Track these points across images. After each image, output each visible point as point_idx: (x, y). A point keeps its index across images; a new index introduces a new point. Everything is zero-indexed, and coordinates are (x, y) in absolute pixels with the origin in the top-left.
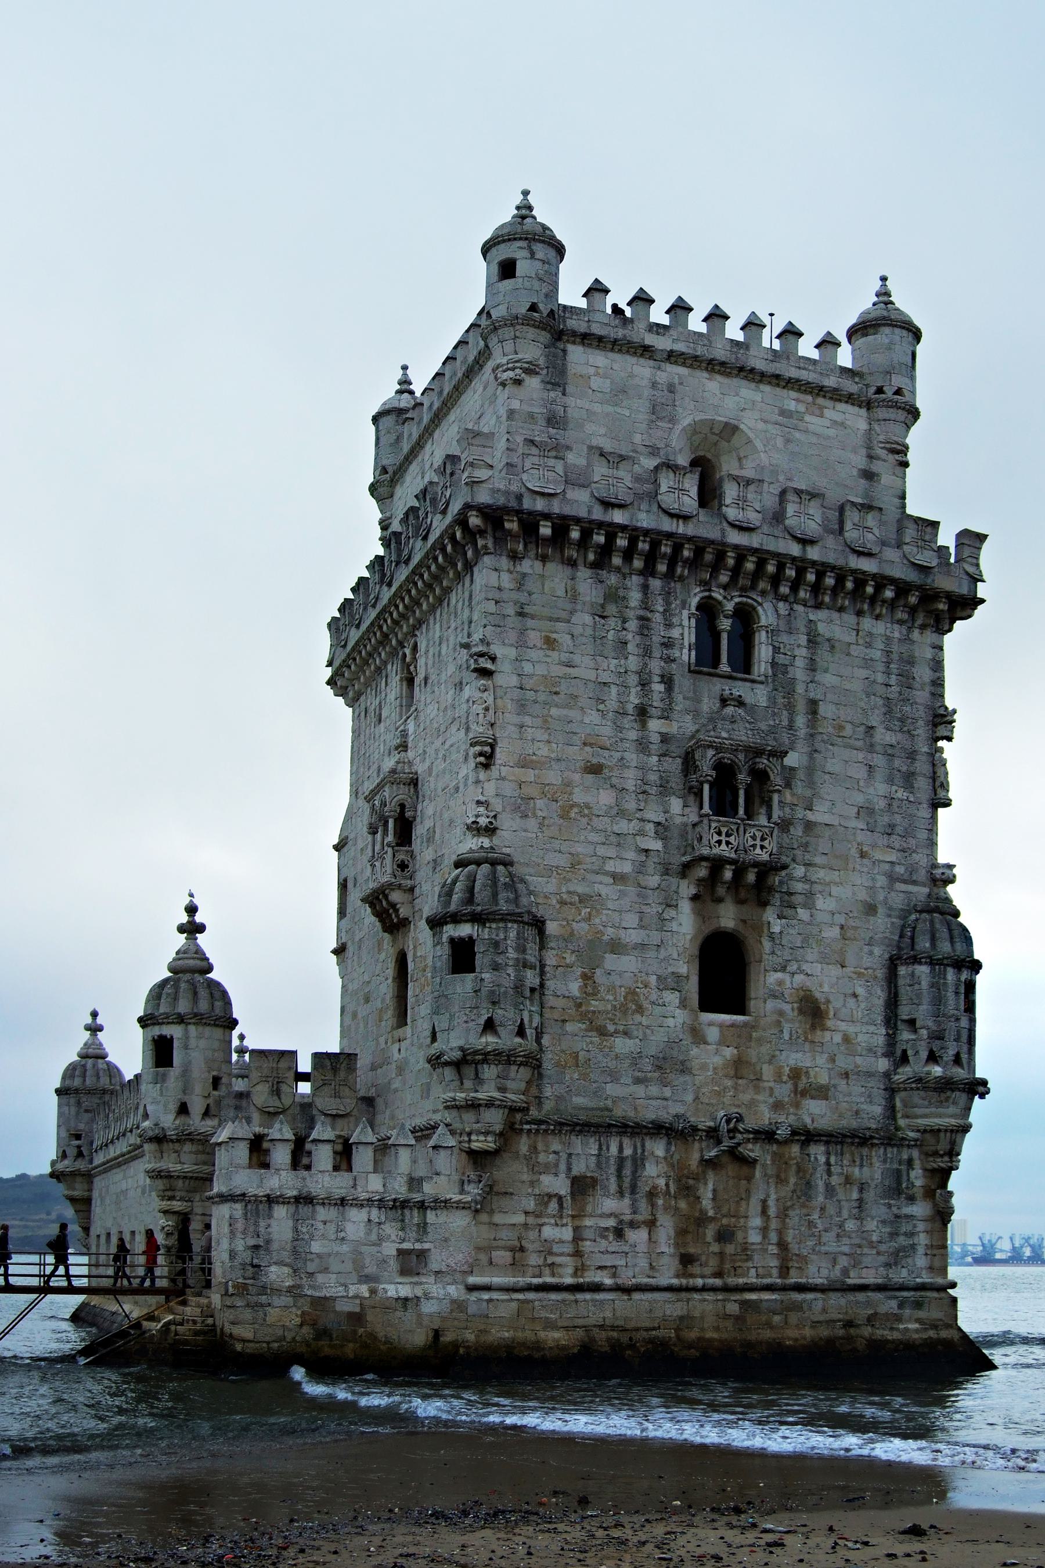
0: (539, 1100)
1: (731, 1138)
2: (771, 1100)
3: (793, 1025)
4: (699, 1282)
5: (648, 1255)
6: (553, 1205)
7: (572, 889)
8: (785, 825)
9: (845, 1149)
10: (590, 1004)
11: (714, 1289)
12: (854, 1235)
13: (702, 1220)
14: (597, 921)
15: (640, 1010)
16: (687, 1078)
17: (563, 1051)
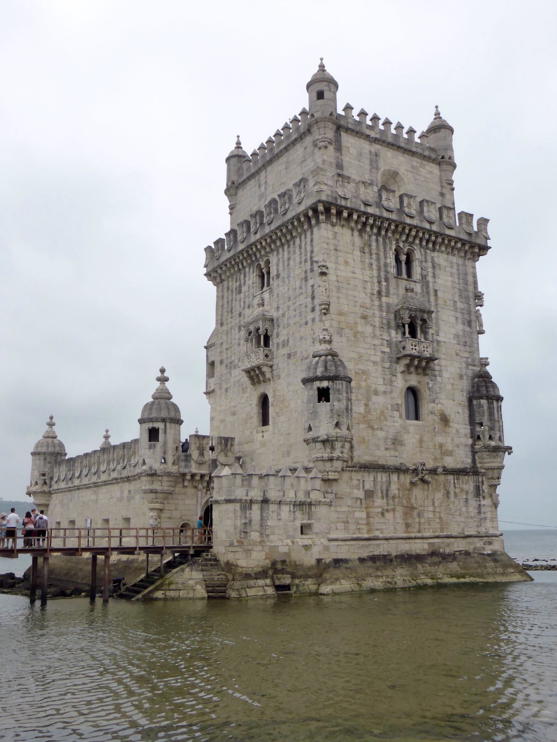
0: (352, 458)
2: (433, 457)
3: (438, 426)
4: (413, 535)
11: (418, 538)
13: (413, 508)
14: (368, 381)
15: (386, 419)
16: (403, 448)
17: (359, 436)
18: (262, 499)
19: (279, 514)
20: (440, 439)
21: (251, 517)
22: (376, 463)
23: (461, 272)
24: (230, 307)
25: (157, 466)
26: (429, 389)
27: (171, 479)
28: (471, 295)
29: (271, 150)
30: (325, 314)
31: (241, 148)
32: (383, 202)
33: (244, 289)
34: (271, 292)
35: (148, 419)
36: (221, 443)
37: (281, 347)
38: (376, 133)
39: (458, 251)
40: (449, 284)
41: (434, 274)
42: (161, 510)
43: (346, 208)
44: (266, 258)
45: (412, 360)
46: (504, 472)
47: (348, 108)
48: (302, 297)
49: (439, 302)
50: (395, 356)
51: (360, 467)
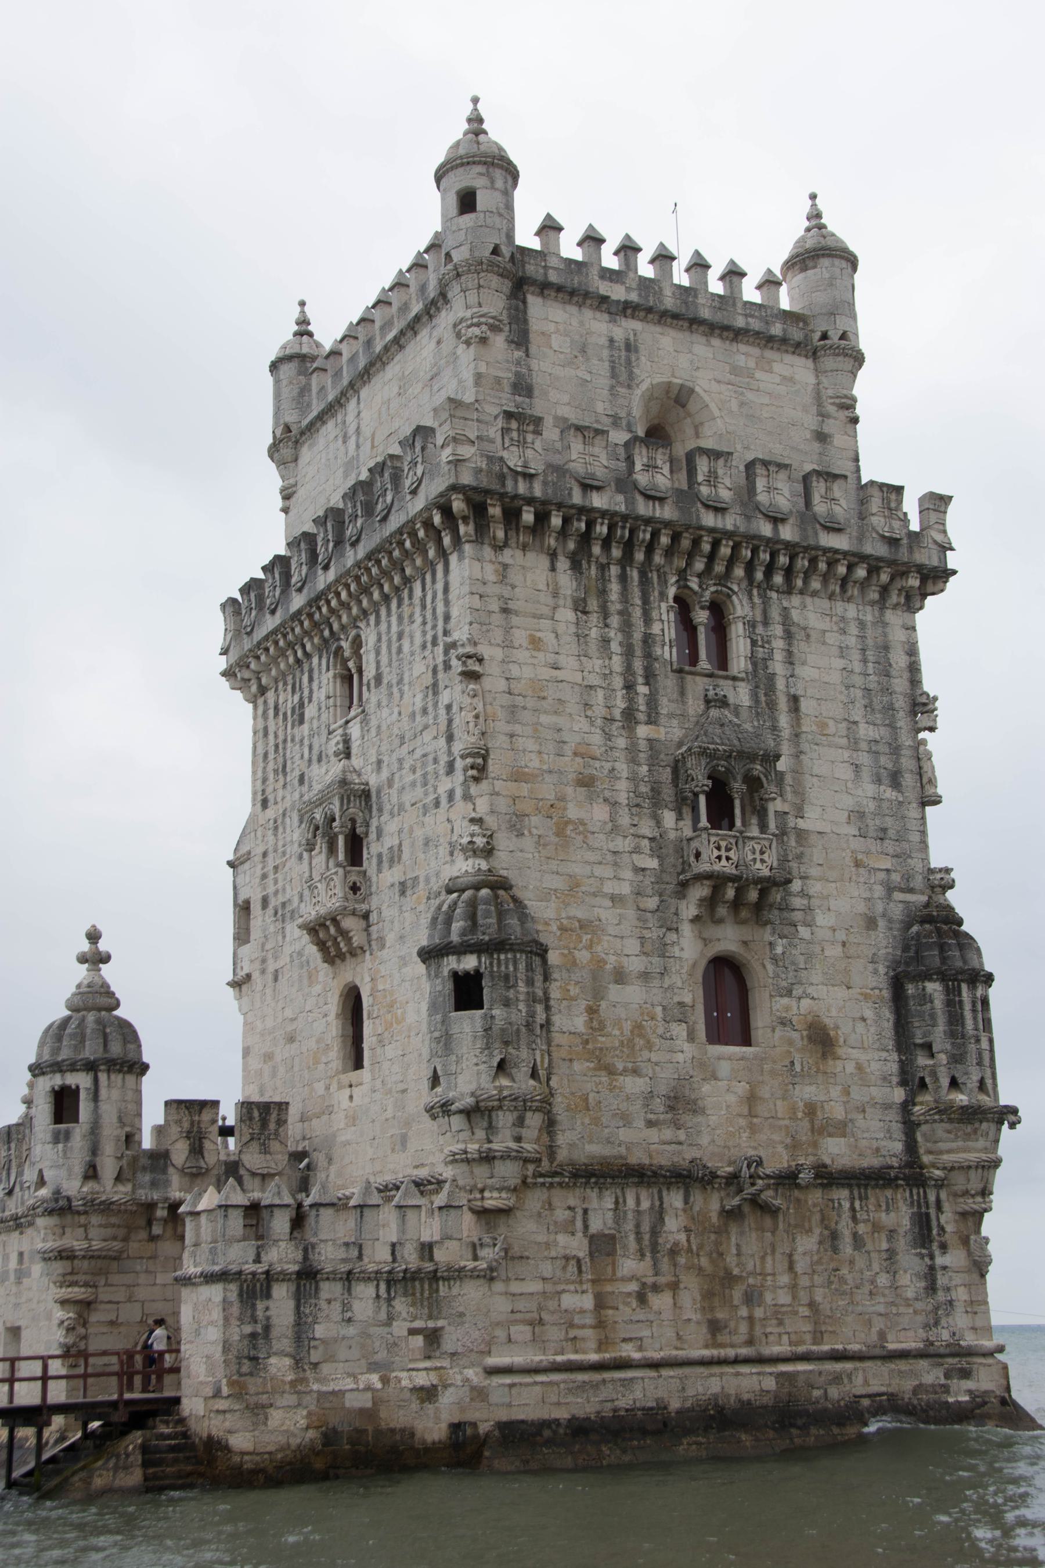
0: (552, 1151)
1: (753, 1184)
4: (731, 1353)
6: (572, 1268)
7: (571, 914)
8: (783, 833)
9: (869, 1191)
11: (747, 1361)
12: (887, 1292)
13: (729, 1279)
14: (599, 948)
15: (649, 1046)
16: (700, 1119)
17: (573, 1093)
18: (295, 1268)
19: (346, 1307)
20: (807, 1092)
21: (268, 1318)
22: (621, 1161)
23: (870, 642)
24: (280, 760)
25: (73, 1187)
26: (775, 960)
27: (113, 1220)
28: (901, 703)
29: (369, 343)
30: (477, 780)
31: (310, 334)
33: (310, 711)
34: (365, 722)
35: (51, 1066)
36: (251, 1119)
37: (386, 865)
38: (628, 289)
40: (835, 677)
41: (790, 653)
43: (530, 501)
44: (353, 633)
46: (1001, 1178)
47: (550, 228)
48: (427, 736)
49: (804, 729)
51: (575, 1176)
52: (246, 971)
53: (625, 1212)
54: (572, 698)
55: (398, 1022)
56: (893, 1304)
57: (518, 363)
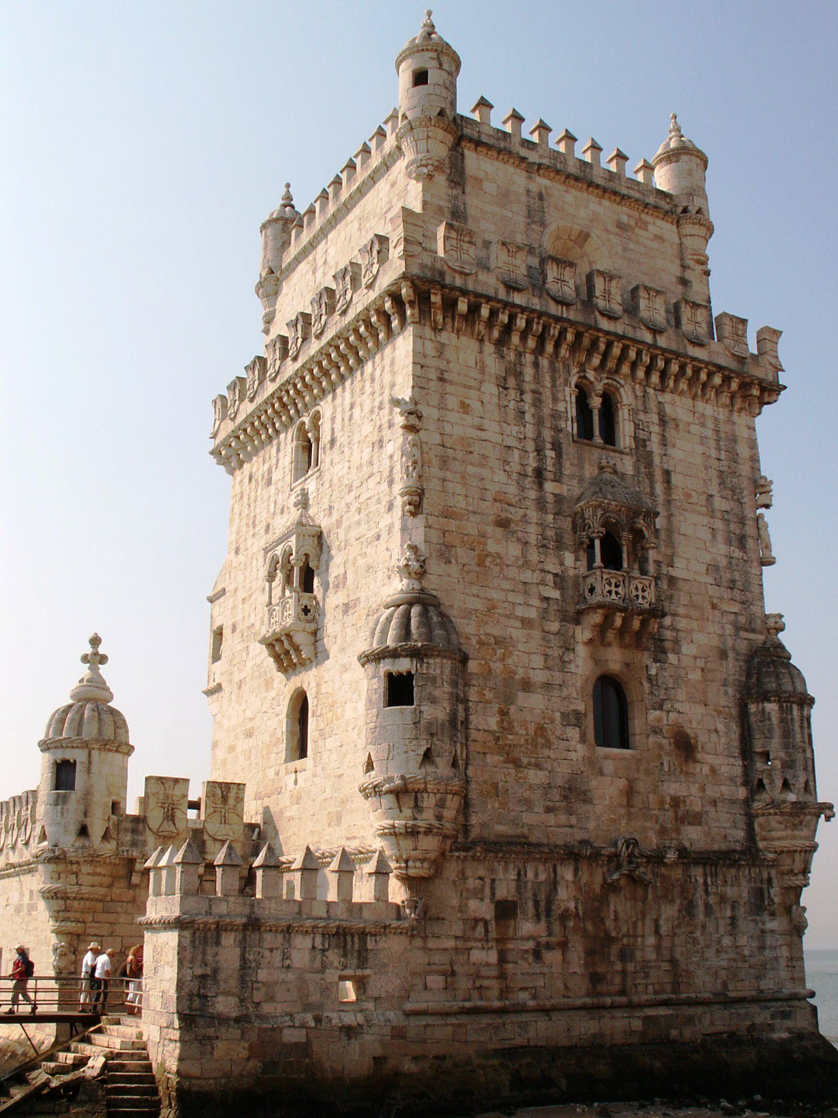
2: (658, 827)
4: (608, 1000)
5: (560, 973)
6: (480, 929)
9: (719, 869)
10: (507, 738)
11: (620, 1006)
12: (730, 950)
13: (609, 940)
14: (510, 661)
15: (548, 745)
16: (588, 807)
17: (485, 782)
19: (286, 956)
23: (722, 435)
26: (649, 678)
28: (746, 484)
31: (293, 207)
32: (547, 286)
39: (717, 394)
40: (698, 460)
42: (79, 935)
43: (464, 292)
45: (608, 619)
48: (372, 483)
50: (571, 609)
52: (217, 681)
53: (526, 883)
54: (493, 455)
55: (338, 719)
56: (735, 960)
57: (456, 198)
